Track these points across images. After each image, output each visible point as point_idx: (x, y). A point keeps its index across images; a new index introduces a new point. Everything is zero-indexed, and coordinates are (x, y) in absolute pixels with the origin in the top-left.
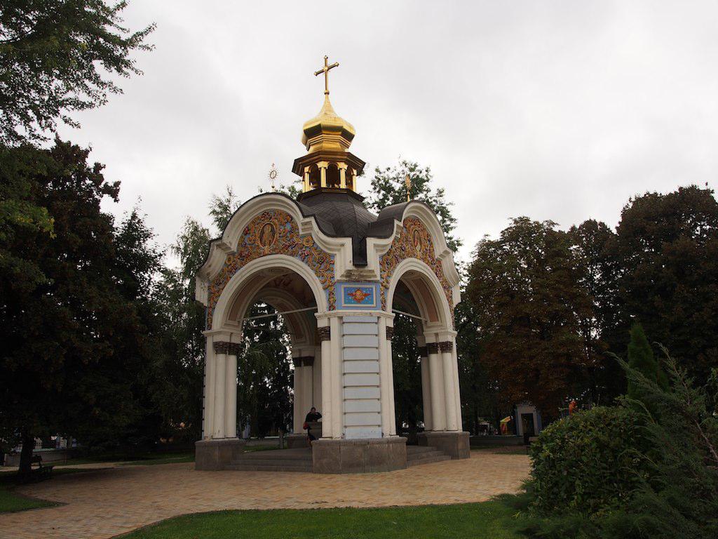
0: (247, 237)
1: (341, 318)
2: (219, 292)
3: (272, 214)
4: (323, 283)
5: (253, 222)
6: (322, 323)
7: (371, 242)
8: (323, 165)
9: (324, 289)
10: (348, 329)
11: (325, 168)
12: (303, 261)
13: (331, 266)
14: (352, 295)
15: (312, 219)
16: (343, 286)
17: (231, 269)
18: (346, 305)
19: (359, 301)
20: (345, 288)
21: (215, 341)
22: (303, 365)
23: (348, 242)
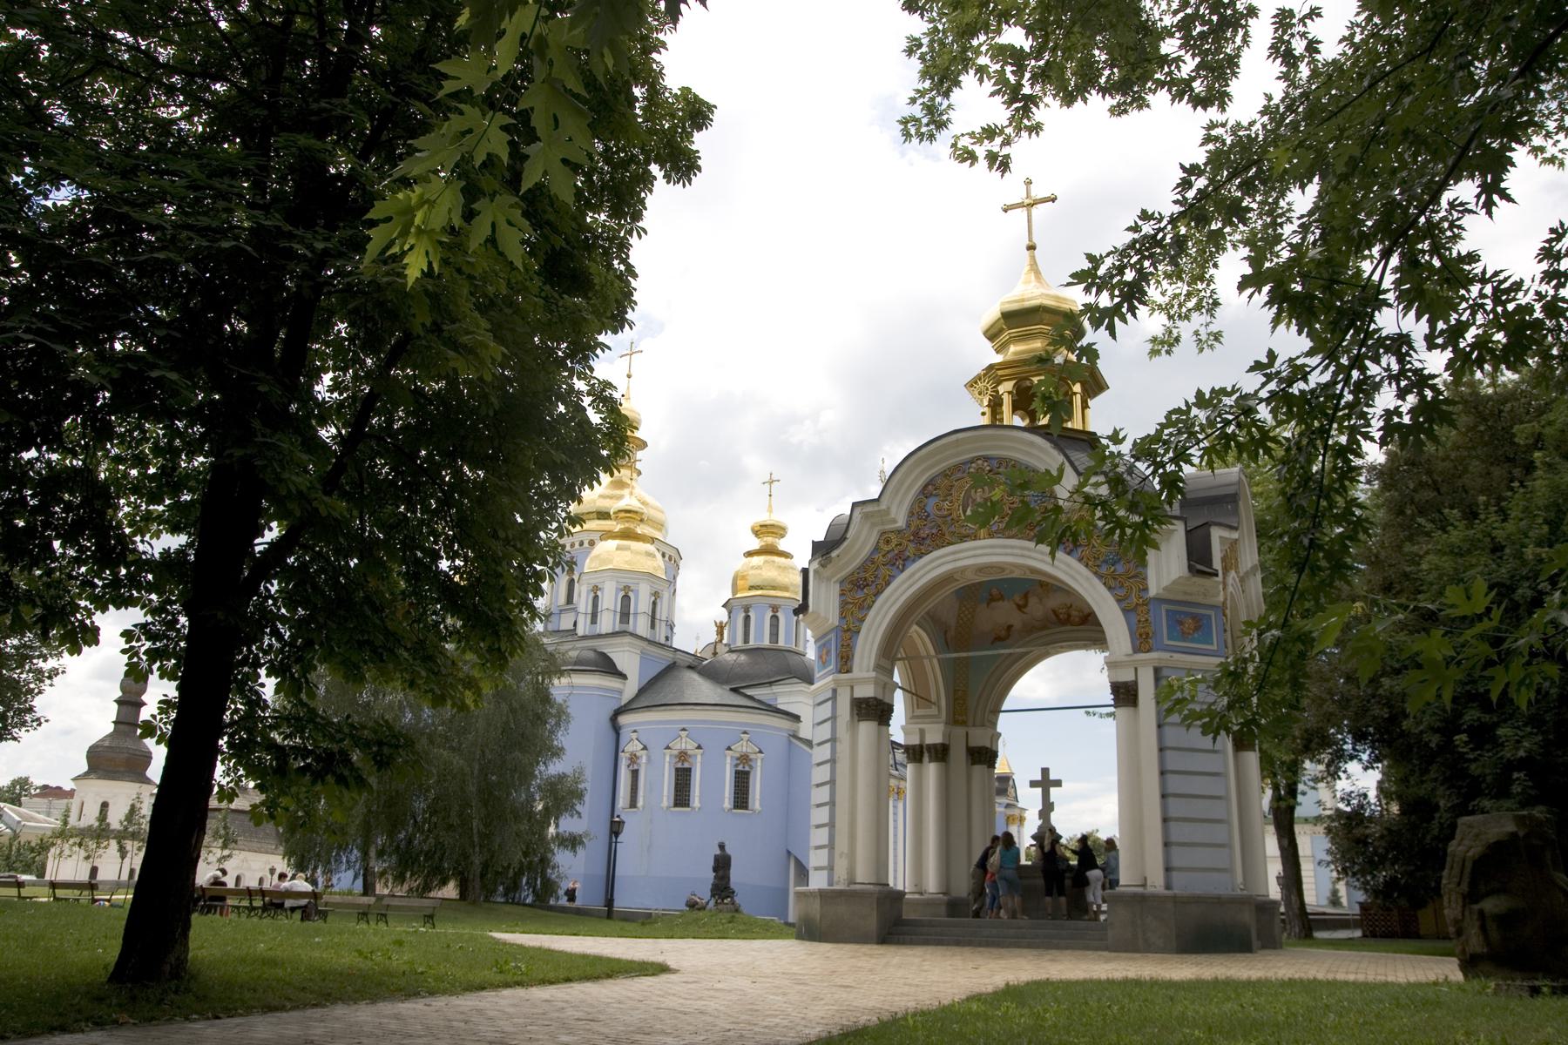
0: (931, 504)
1: (1157, 671)
5: (945, 474)
7: (1217, 534)
12: (1069, 554)
13: (1140, 569)
16: (1164, 607)
17: (900, 561)
20: (1167, 611)
21: (856, 695)
22: (926, 758)
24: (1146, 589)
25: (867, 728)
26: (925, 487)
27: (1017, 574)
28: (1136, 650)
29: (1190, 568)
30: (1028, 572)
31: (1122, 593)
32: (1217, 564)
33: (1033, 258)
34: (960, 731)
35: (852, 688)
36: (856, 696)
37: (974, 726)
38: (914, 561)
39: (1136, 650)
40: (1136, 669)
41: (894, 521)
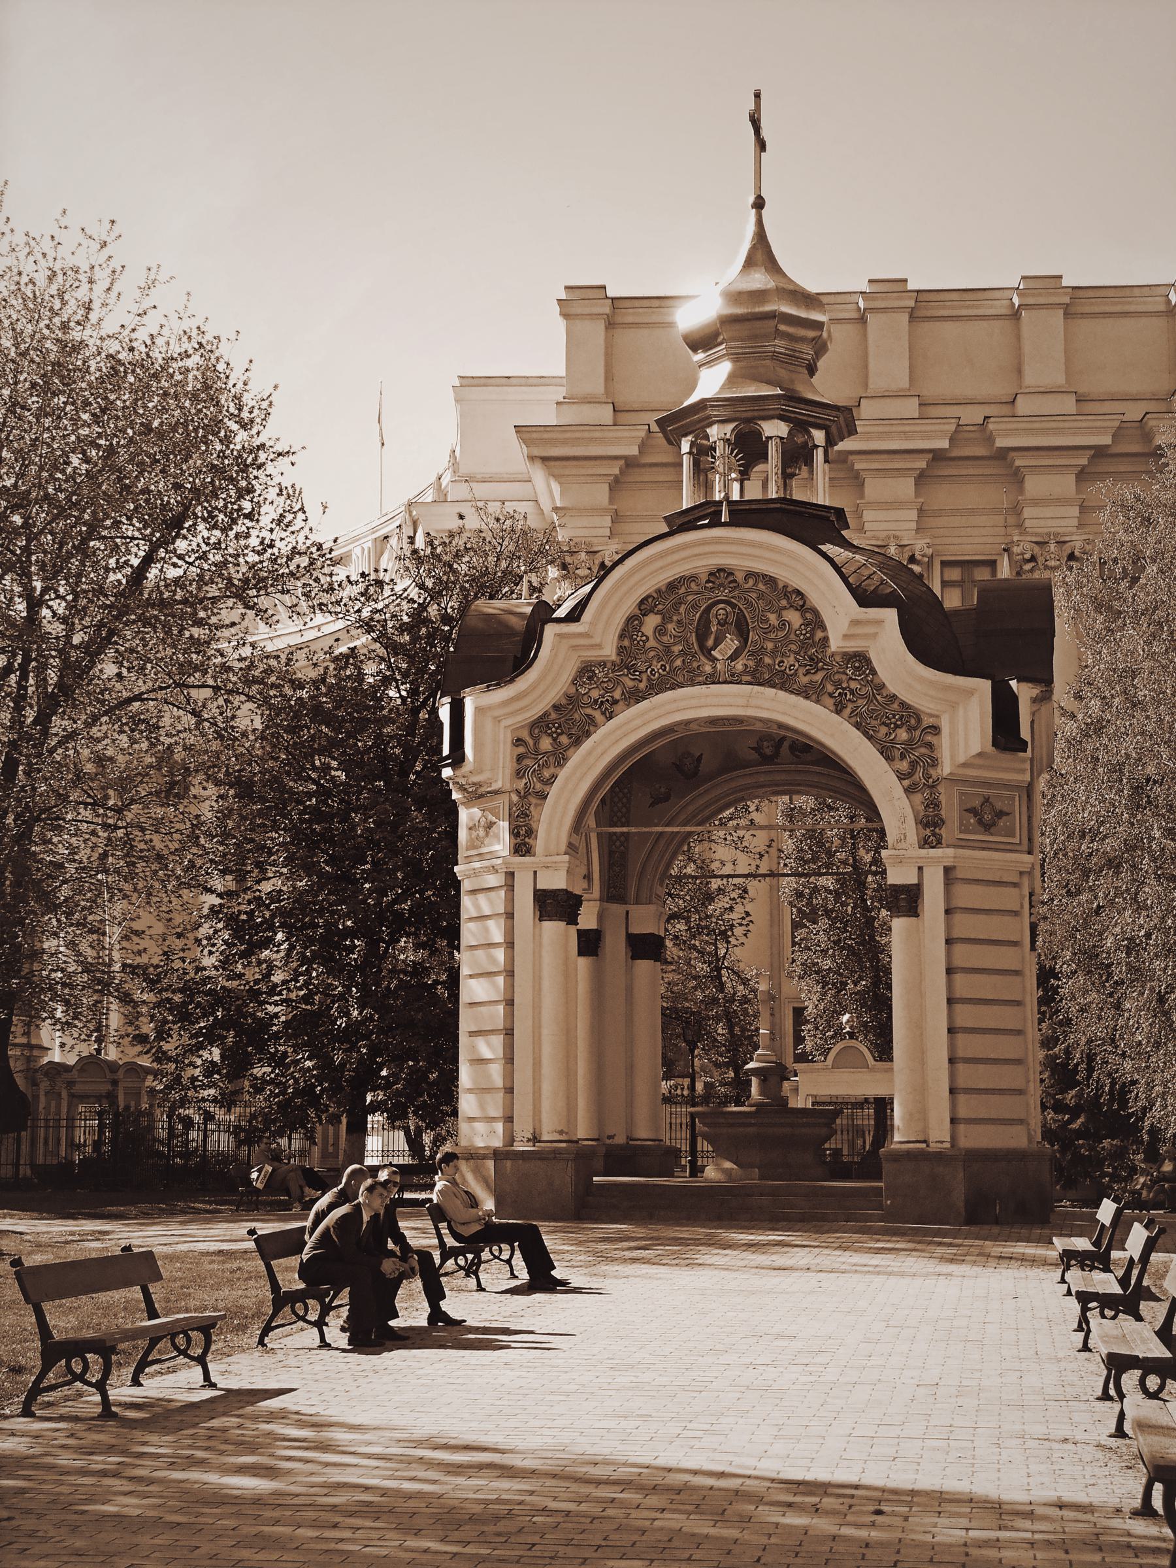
2: (560, 758)
3: (740, 577)
4: (901, 776)
5: (672, 586)
6: (897, 876)
8: (775, 429)
9: (908, 791)
10: (966, 896)
11: (781, 438)
12: (838, 712)
13: (929, 738)
14: (973, 811)
15: (890, 615)
18: (963, 836)
19: (987, 827)
20: (961, 794)
23: (983, 687)
24: (934, 763)
25: (553, 929)
26: (642, 602)
27: (758, 726)
28: (925, 843)
29: (995, 743)
30: (775, 727)
31: (904, 766)
32: (1025, 733)
33: (760, 222)
34: (617, 909)
35: (535, 873)
36: (539, 887)
37: (637, 902)
38: (629, 706)
39: (925, 843)
40: (920, 869)
41: (599, 646)
